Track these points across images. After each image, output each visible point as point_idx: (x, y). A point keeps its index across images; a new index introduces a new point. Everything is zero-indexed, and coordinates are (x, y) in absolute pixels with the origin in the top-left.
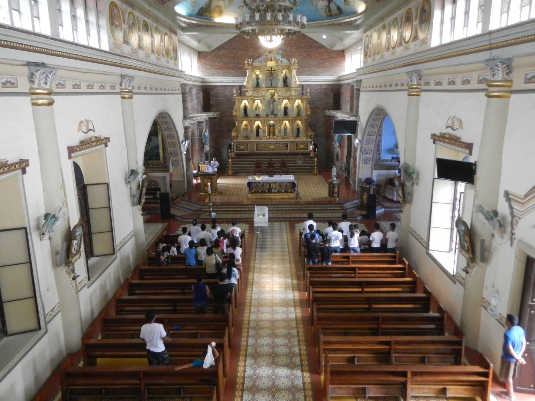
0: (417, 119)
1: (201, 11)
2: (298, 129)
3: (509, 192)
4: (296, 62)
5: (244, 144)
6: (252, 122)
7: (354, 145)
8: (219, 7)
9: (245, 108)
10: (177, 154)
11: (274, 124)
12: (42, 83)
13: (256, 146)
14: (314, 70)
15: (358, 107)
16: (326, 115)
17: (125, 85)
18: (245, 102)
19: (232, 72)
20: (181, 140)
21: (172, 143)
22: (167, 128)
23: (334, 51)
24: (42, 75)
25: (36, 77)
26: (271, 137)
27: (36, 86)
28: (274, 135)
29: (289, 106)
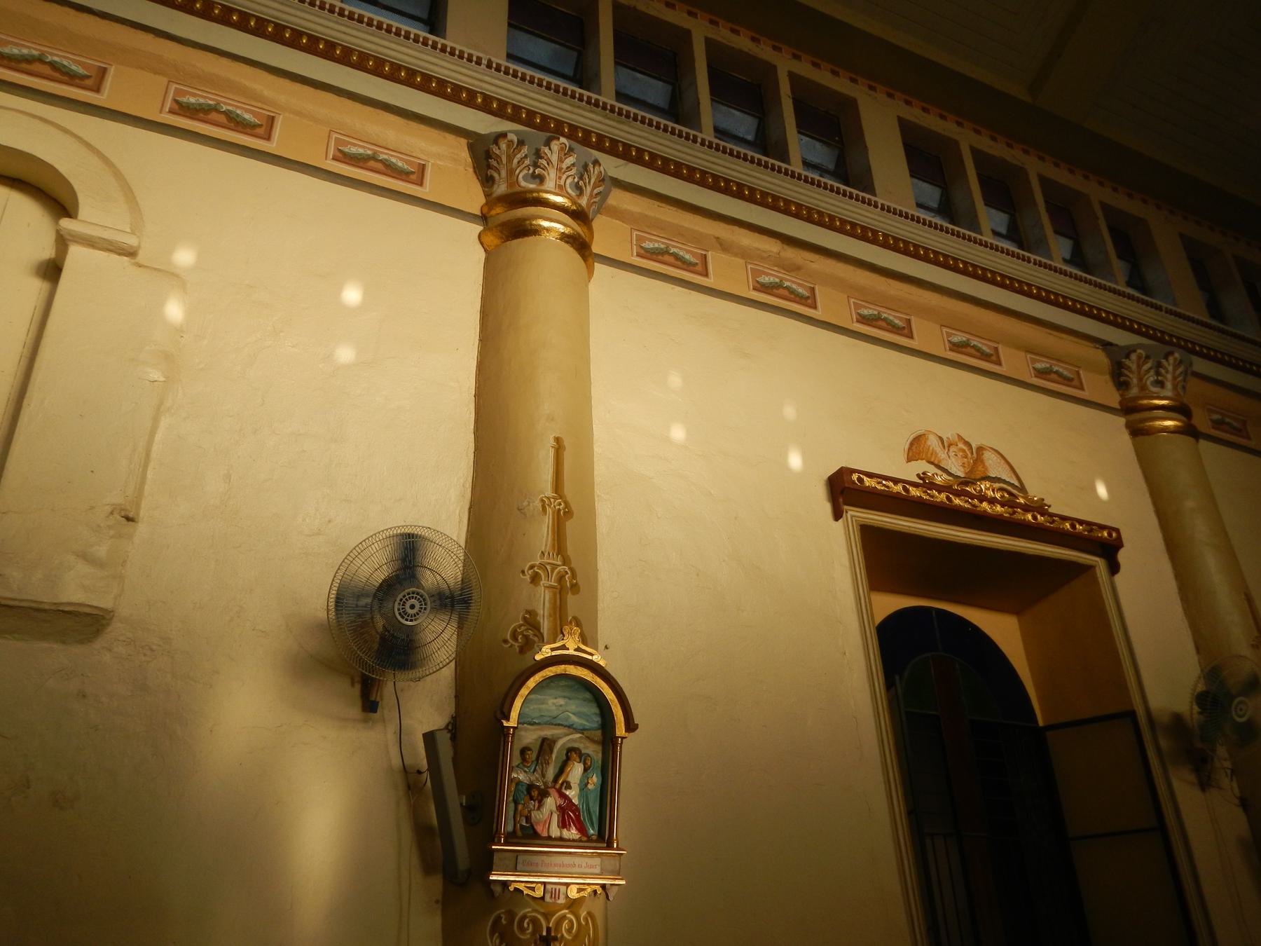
12: (1148, 383)
24: (1145, 362)
25: (1131, 371)
27: (1134, 391)
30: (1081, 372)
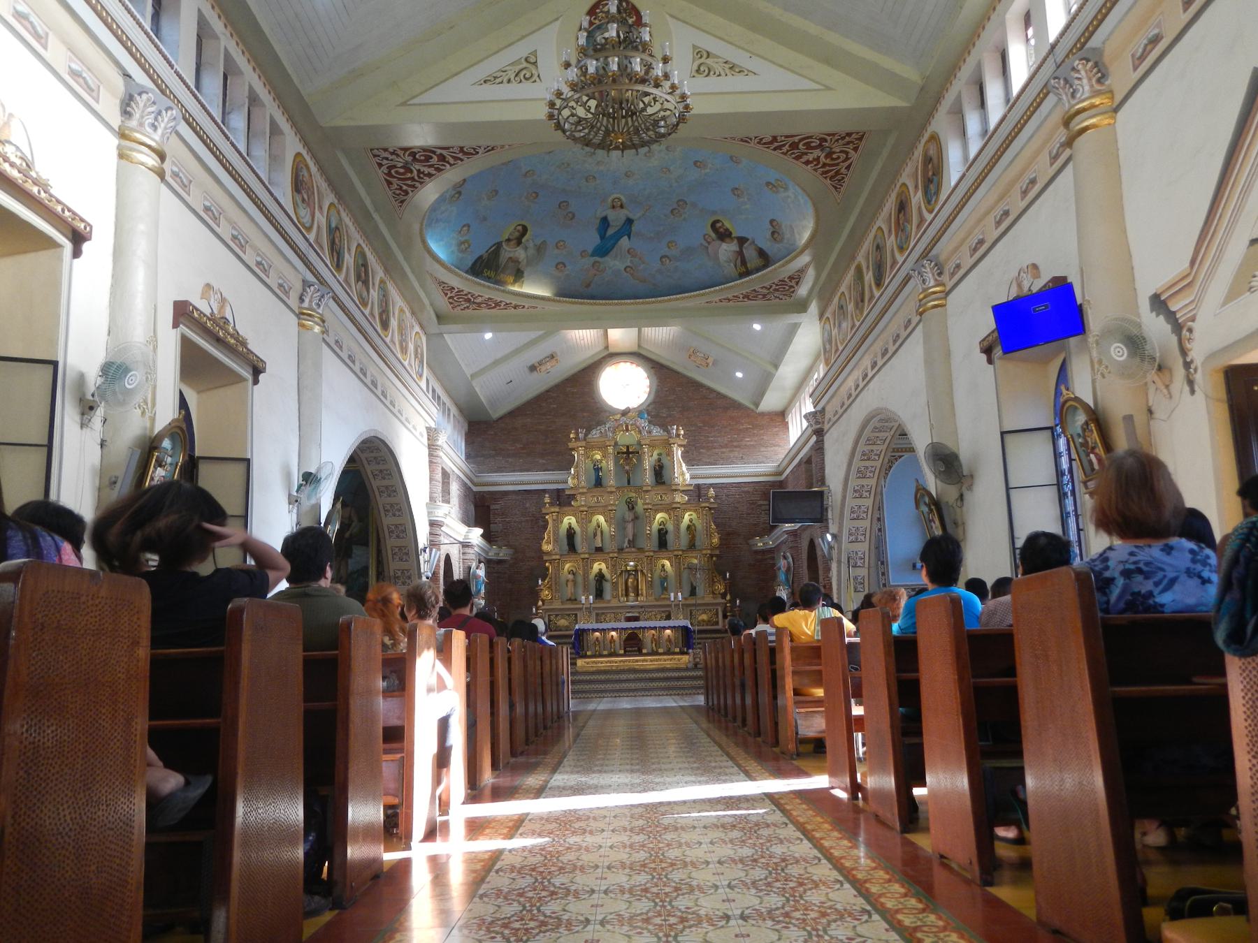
0: (948, 354)
1: (478, 265)
3: (1158, 293)
4: (682, 432)
5: (569, 615)
6: (587, 564)
7: (824, 556)
8: (516, 261)
9: (571, 534)
10: (409, 578)
11: (636, 566)
14: (723, 453)
15: (822, 469)
16: (755, 548)
17: (311, 301)
18: (569, 520)
19: (541, 461)
20: (421, 546)
21: (400, 548)
22: (392, 505)
23: (763, 414)
24: (150, 106)
27: (133, 123)
28: (637, 595)
29: (670, 527)
30: (101, 88)
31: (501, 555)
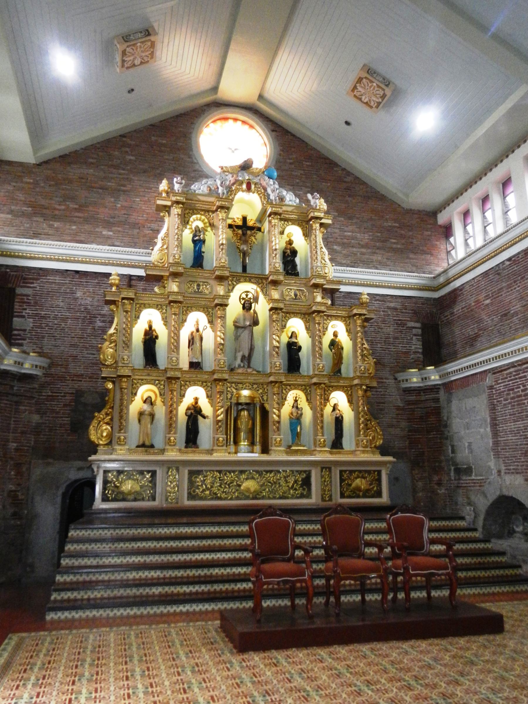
2: (339, 421)
11: (252, 398)
13: (191, 483)
14: (363, 254)
19: (105, 233)
26: (244, 444)
31: (27, 365)
